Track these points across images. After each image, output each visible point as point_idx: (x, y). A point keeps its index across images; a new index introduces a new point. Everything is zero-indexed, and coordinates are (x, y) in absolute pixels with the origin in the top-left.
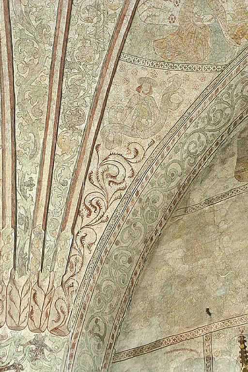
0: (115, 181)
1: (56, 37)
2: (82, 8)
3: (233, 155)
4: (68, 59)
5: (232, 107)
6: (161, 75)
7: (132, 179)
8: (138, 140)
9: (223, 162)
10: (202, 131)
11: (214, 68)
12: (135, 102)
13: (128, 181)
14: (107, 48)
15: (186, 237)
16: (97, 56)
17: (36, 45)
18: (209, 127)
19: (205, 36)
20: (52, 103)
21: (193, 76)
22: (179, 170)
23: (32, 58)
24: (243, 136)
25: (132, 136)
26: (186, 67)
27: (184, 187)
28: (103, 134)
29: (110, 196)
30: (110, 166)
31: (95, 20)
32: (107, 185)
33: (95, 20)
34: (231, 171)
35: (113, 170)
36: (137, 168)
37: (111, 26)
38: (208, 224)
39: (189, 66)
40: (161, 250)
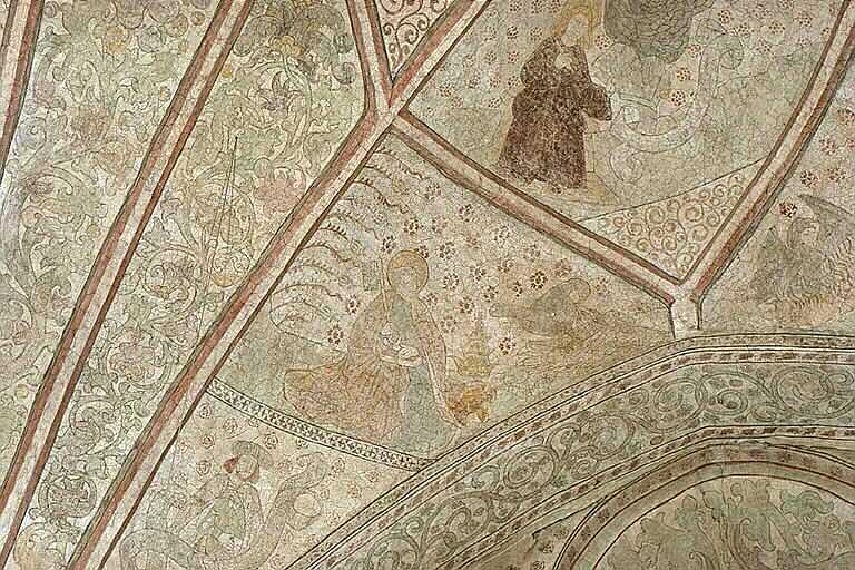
1: (79, 311)
2: (155, 262)
4: (92, 363)
5: (420, 551)
6: (286, 444)
11: (402, 461)
12: (215, 491)
14: (184, 360)
16: (159, 372)
17: (26, 315)
19: (396, 390)
20: (29, 454)
23: (11, 341)
26: (343, 443)
28: (125, 550)
31: (174, 296)
33: (174, 296)
37: (207, 317)
39: (349, 443)
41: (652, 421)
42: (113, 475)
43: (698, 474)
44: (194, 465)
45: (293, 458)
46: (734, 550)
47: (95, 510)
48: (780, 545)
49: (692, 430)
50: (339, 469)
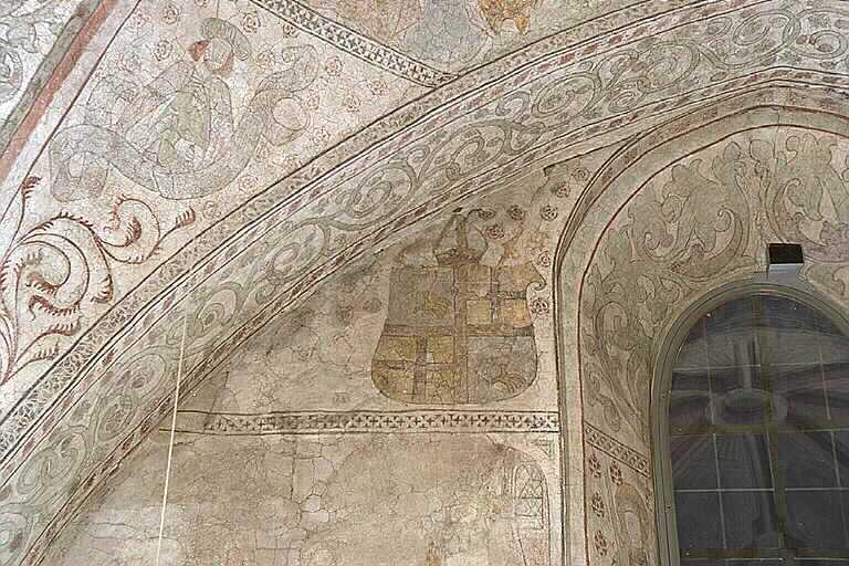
0: (51, 300)
3: (373, 307)
5: (416, 182)
7: (104, 308)
8: (152, 196)
9: (343, 315)
10: (325, 224)
11: (414, 70)
12: (175, 82)
13: (90, 312)
15: (196, 507)
18: (345, 219)
21: (352, 66)
22: (230, 309)
24: (409, 259)
25: (137, 179)
27: (219, 353)
29: (24, 342)
30: (46, 250)
32: (24, 309)
34: (363, 354)
35: (53, 267)
36: (124, 279)
38: (269, 490)
39: (351, 38)
40: (113, 521)
41: (723, 54)
42: (46, 49)
43: (749, 117)
44: (151, 46)
45: (278, 48)
46: (771, 211)
47: (20, 94)
48: (830, 216)
49: (763, 68)
50: (334, 70)
